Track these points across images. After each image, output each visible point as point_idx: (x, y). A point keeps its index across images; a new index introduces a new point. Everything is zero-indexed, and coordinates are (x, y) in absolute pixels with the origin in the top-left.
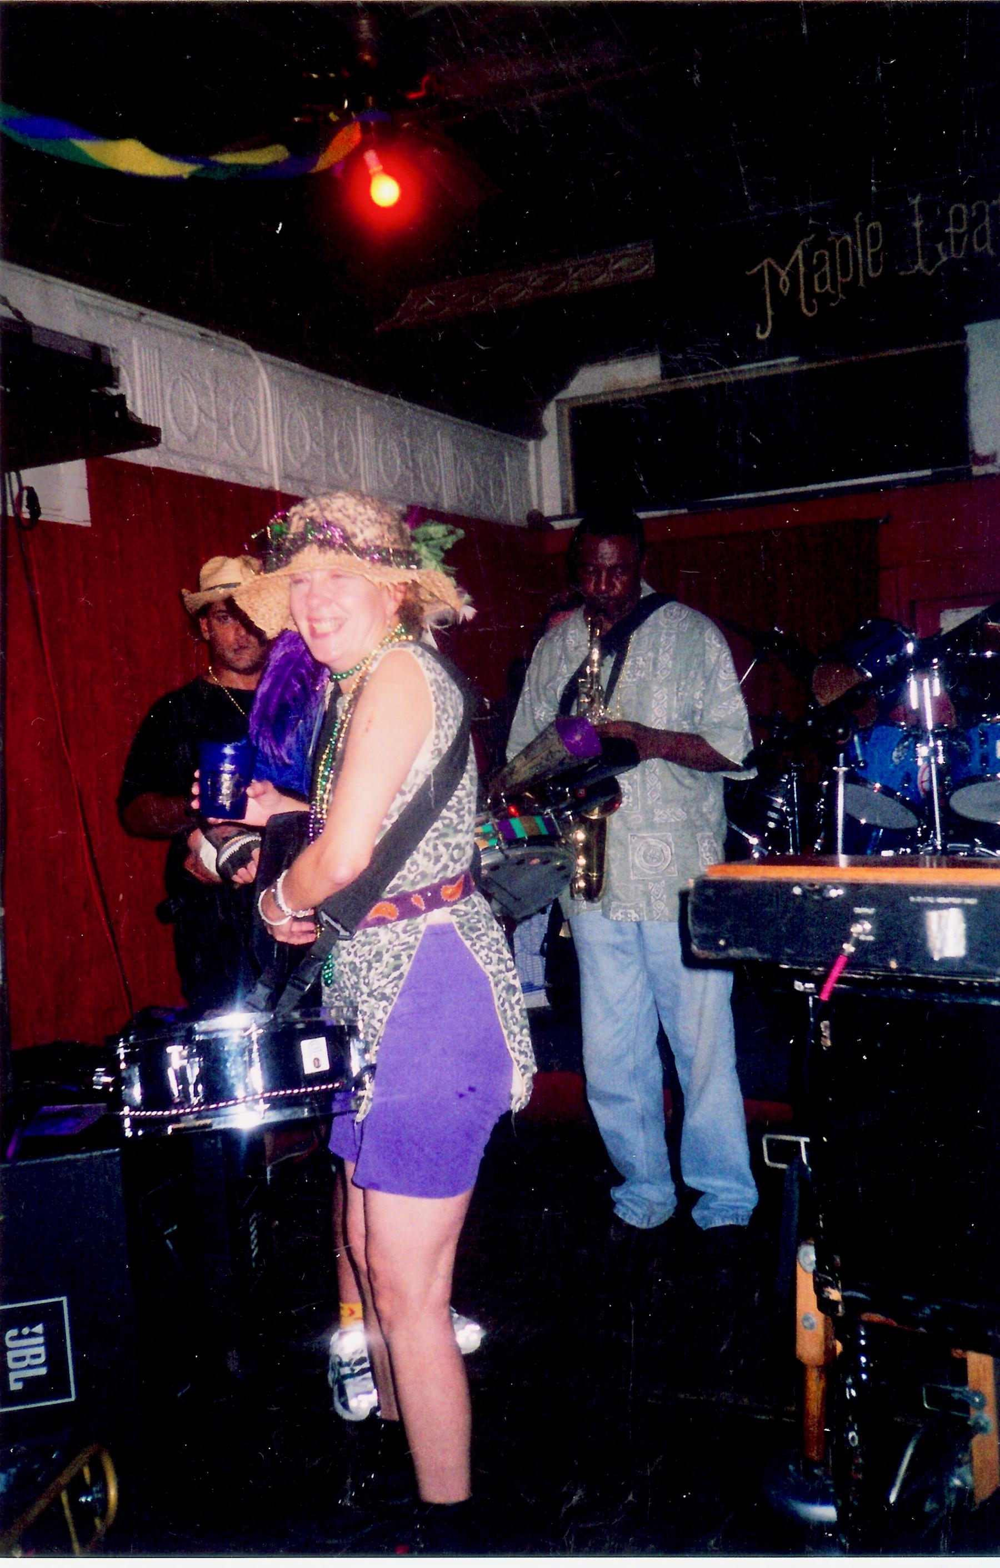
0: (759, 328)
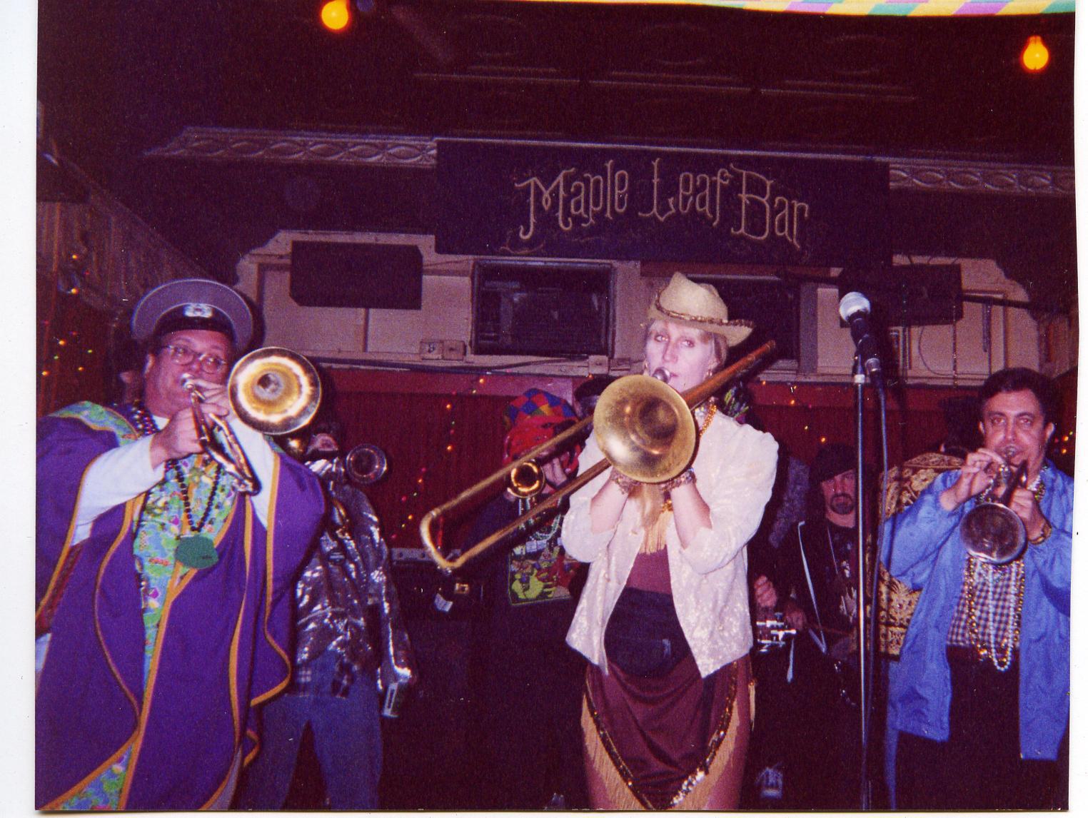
0: (522, 228)
